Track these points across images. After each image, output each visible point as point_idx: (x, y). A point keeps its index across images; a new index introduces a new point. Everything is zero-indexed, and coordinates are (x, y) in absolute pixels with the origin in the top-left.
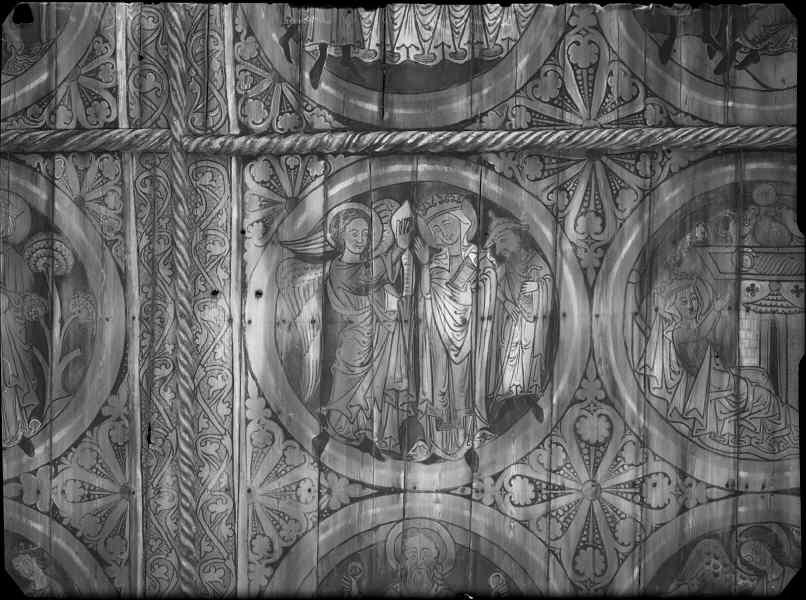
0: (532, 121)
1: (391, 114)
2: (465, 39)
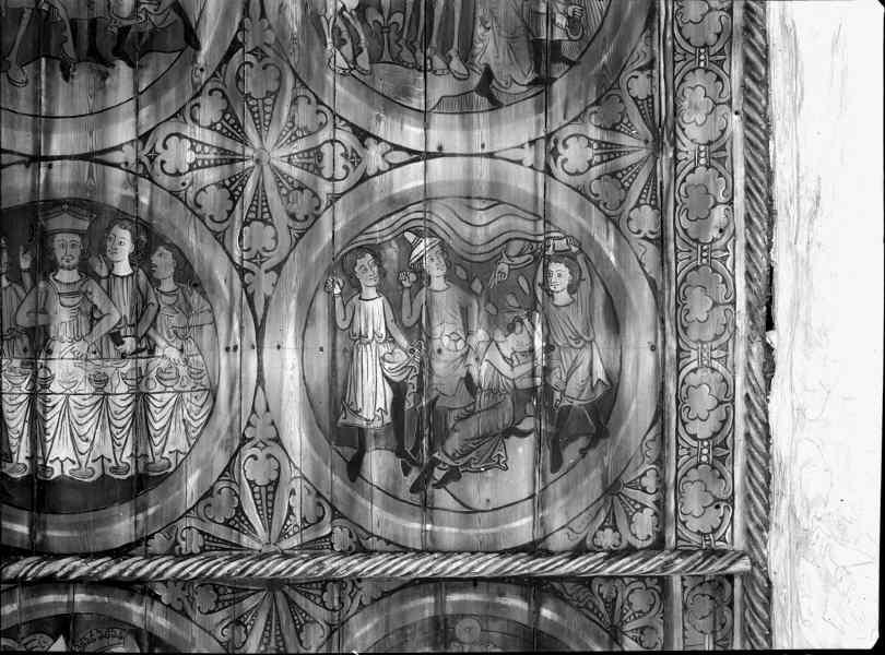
0: (205, 545)
1: (44, 536)
2: (128, 451)
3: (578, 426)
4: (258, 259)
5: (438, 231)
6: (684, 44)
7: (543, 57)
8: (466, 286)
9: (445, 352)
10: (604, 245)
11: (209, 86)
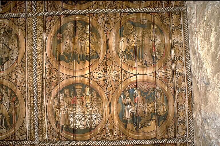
1: (75, 138)
2: (89, 124)
3: (161, 119)
4: (109, 92)
5: (138, 87)
6: (176, 56)
7: (154, 59)
8: (143, 96)
9: (140, 107)
10: (165, 89)
11: (101, 64)
